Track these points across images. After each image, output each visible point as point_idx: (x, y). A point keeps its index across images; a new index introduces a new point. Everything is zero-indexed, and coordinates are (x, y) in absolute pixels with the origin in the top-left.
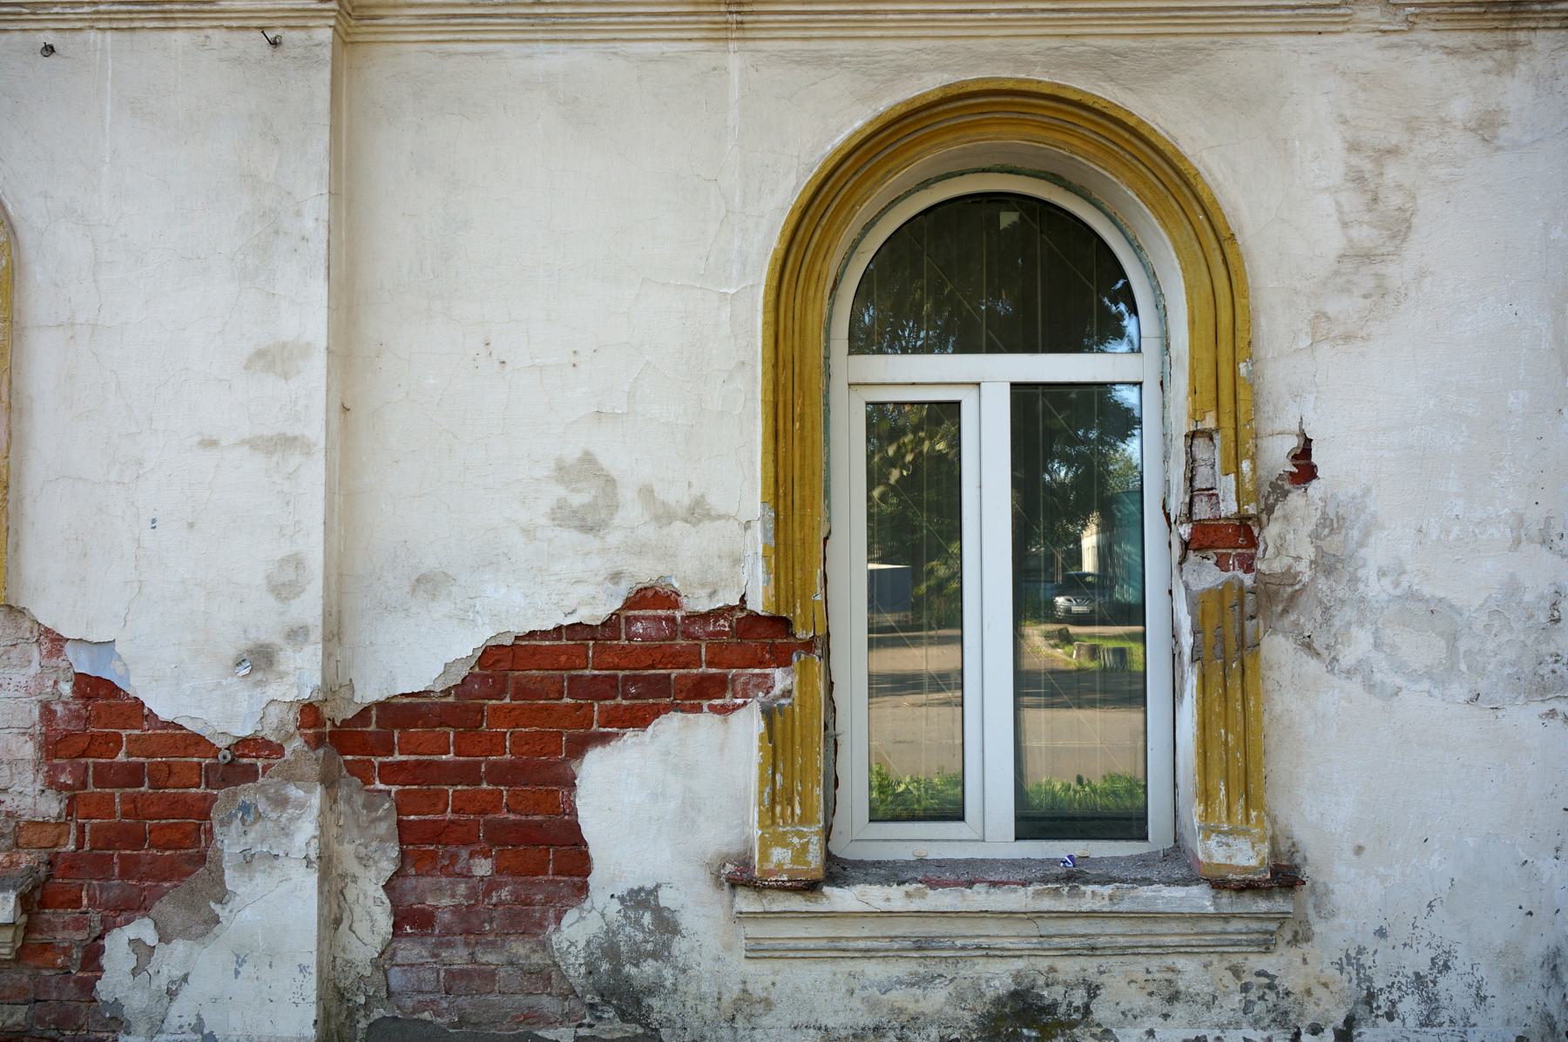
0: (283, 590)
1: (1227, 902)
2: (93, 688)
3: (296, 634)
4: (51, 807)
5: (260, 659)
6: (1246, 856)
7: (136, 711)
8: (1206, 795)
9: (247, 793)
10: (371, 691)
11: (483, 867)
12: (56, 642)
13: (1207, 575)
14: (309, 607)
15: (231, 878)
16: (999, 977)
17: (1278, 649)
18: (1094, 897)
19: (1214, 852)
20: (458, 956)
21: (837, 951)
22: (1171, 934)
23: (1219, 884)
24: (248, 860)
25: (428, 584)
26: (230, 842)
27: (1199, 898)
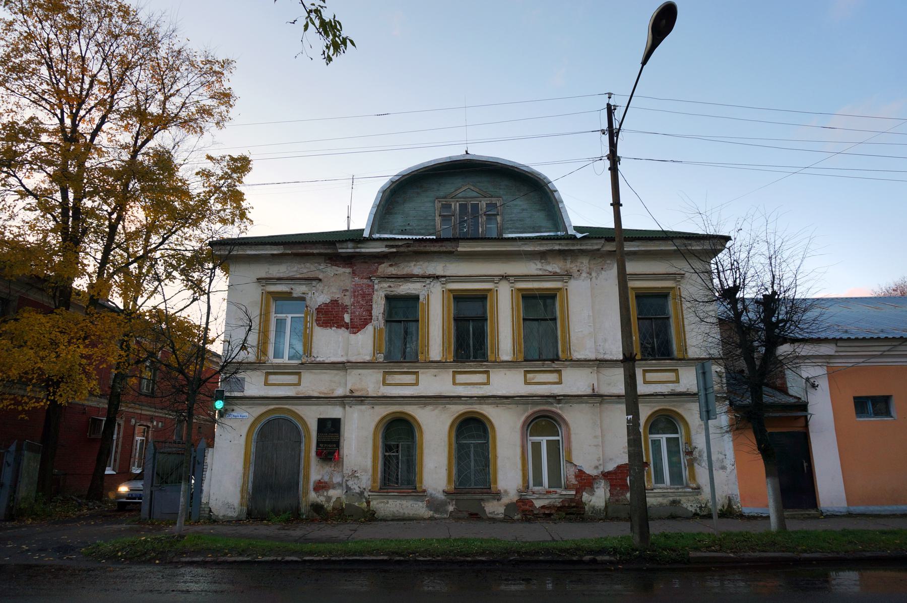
0: (599, 460)
1: (693, 491)
2: (580, 471)
3: (600, 465)
4: (576, 483)
5: (596, 467)
6: (695, 486)
7: (584, 473)
8: (690, 480)
9: (596, 481)
10: (606, 471)
11: (618, 489)
12: (576, 465)
13: (688, 457)
14: (601, 462)
15: (595, 489)
16: (671, 499)
17: (695, 465)
18: (680, 490)
19: (691, 485)
20: (616, 498)
21: (655, 497)
22: (688, 494)
23: (692, 489)
24: (597, 488)
25: (611, 459)
26: (595, 486)
27: (690, 490)
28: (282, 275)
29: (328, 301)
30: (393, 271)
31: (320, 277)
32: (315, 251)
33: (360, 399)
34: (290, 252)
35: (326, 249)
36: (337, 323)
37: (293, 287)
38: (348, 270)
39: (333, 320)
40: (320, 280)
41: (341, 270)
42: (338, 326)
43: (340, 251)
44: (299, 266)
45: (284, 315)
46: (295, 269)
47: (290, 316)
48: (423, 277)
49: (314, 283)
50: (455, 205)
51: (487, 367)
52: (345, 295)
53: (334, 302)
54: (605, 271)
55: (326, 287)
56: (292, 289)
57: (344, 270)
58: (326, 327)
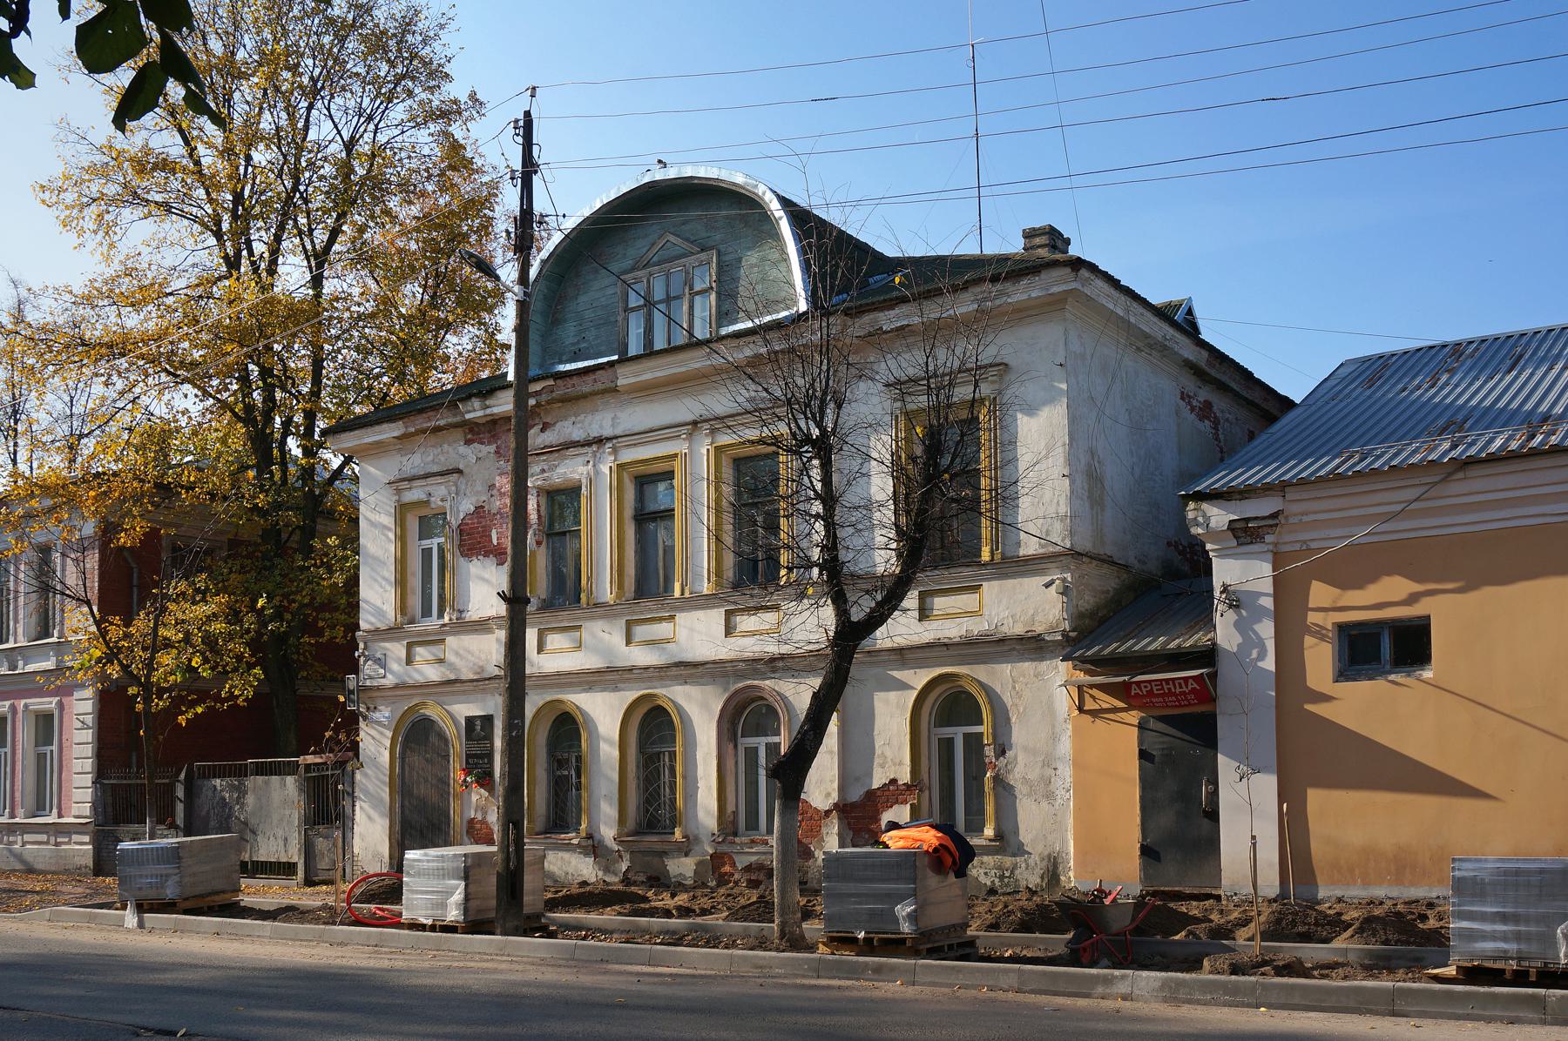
28: (416, 472)
29: (473, 509)
30: (550, 437)
32: (442, 423)
34: (413, 430)
36: (485, 547)
38: (492, 448)
39: (479, 542)
40: (459, 471)
42: (485, 552)
43: (468, 416)
48: (587, 443)
51: (673, 609)
52: (492, 496)
53: (479, 509)
58: (472, 555)
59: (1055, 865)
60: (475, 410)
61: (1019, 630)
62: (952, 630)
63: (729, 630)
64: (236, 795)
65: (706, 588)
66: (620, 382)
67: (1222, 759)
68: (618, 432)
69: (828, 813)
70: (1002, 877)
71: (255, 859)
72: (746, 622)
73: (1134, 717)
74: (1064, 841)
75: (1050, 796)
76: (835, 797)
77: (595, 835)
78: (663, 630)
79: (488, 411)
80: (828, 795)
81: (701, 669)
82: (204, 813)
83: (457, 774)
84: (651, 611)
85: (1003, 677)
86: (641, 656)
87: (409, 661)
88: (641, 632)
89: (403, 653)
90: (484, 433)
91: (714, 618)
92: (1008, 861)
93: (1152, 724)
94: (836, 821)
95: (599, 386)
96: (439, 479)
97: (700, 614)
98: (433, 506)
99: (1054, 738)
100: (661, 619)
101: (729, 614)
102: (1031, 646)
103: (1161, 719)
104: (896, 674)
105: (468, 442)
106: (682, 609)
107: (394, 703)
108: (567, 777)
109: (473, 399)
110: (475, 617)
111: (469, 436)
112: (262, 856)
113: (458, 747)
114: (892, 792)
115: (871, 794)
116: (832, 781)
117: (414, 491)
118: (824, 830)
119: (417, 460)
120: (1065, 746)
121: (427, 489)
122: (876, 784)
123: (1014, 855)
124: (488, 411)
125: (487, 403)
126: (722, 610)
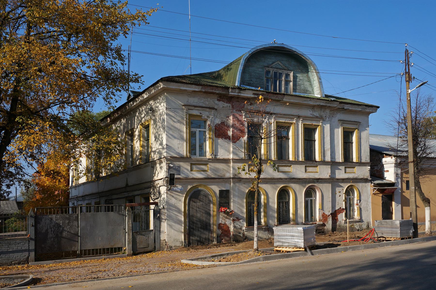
28: (195, 104)
31: (216, 107)
33: (237, 179)
35: (223, 91)
36: (225, 136)
37: (202, 112)
41: (226, 105)
42: (225, 137)
44: (204, 100)
45: (195, 129)
46: (202, 101)
47: (198, 130)
49: (213, 111)
50: (272, 72)
53: (223, 123)
54: (334, 118)
55: (218, 114)
56: (201, 113)
57: (227, 104)
59: (369, 224)
60: (235, 92)
61: (362, 177)
62: (351, 176)
63: (306, 171)
64: (67, 222)
65: (300, 159)
66: (284, 100)
67: (393, 203)
68: (275, 112)
69: (329, 215)
70: (360, 227)
71: (83, 249)
72: (310, 169)
73: (381, 195)
74: (370, 219)
75: (367, 210)
76: (331, 212)
77: (268, 225)
78: (286, 169)
79: (240, 94)
80: (329, 211)
81: (301, 180)
82: (44, 231)
83: (213, 209)
84: (286, 163)
85: (360, 185)
86: (282, 176)
87: (192, 170)
88: (281, 168)
89: (189, 168)
90: (224, 99)
91: (302, 167)
92: (361, 223)
93: (383, 196)
94: (331, 217)
95: (277, 99)
96: (208, 110)
97: (299, 166)
98: (203, 118)
99: (368, 199)
100: (287, 166)
101: (306, 166)
102: (365, 180)
103: (385, 195)
104: (341, 184)
105: (218, 100)
106: (293, 164)
107: (184, 184)
108: (251, 209)
109: (236, 89)
110: (221, 158)
111: (219, 98)
112: (90, 246)
113: (215, 199)
114: (340, 210)
115: (336, 211)
116: (330, 208)
117: (194, 111)
118: (328, 220)
119: (194, 101)
120: (370, 200)
121: (200, 111)
122: (337, 209)
123: (362, 222)
124: (240, 94)
125: (241, 92)
126: (304, 166)
